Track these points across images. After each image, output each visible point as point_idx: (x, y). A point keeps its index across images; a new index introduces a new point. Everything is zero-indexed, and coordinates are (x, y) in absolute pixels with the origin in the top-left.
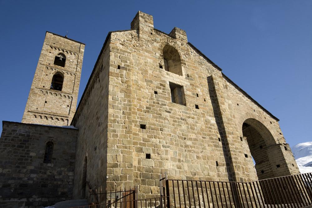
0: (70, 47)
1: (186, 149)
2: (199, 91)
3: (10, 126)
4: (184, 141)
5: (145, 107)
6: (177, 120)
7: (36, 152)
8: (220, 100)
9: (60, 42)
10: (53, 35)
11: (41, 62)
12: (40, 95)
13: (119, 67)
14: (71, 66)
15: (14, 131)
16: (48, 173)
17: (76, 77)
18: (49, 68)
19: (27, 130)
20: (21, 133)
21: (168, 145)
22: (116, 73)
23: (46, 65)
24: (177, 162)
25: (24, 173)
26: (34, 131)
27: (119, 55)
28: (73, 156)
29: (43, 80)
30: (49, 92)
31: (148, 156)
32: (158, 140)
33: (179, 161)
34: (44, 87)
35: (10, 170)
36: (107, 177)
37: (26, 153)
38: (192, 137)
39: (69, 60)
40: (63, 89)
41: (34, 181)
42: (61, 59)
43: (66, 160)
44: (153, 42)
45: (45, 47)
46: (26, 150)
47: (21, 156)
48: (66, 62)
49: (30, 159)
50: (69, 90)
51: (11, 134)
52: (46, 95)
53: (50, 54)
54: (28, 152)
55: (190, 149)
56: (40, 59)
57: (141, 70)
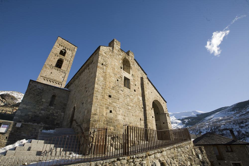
2: (136, 83)
3: (33, 83)
6: (126, 95)
7: (45, 100)
8: (145, 89)
9: (65, 43)
13: (102, 64)
15: (35, 86)
16: (51, 112)
17: (70, 63)
18: (56, 56)
19: (43, 87)
20: (39, 88)
21: (120, 107)
22: (101, 67)
23: (55, 54)
24: (124, 116)
26: (46, 88)
27: (103, 58)
28: (65, 105)
29: (52, 61)
30: (54, 68)
31: (111, 112)
32: (116, 104)
33: (125, 116)
34: (52, 65)
35: (30, 107)
36: (91, 120)
38: (131, 105)
39: (68, 54)
40: (62, 68)
41: (42, 115)
42: (64, 52)
43: (61, 106)
44: (119, 55)
45: (56, 44)
46: (40, 97)
47: (37, 100)
48: (66, 54)
49: (42, 102)
50: (65, 69)
51: (33, 87)
52: (52, 69)
56: (52, 50)
57: (112, 68)
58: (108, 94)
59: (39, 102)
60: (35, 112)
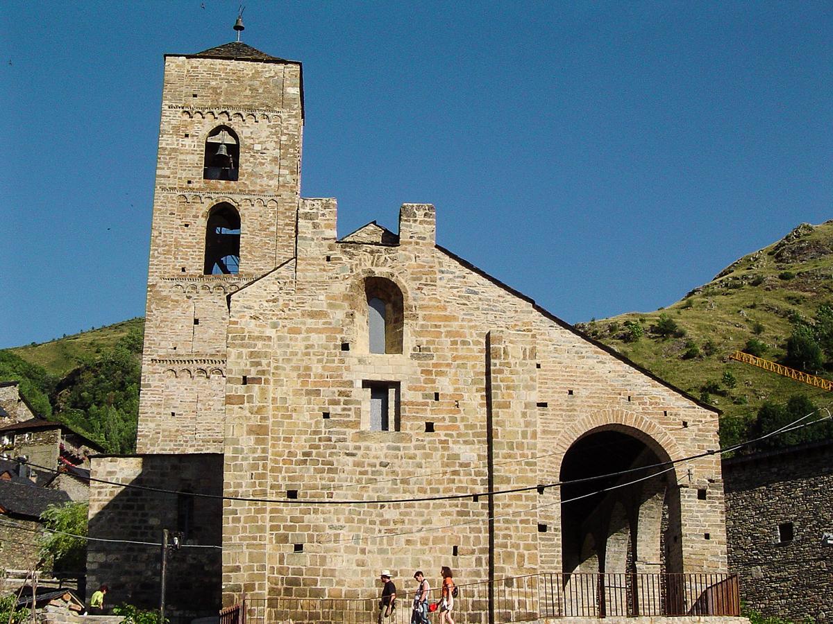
0: (248, 92)
1: (381, 527)
2: (445, 385)
4: (381, 511)
5: (299, 453)
6: (370, 469)
9: (213, 83)
10: (187, 60)
11: (162, 180)
12: (177, 301)
14: (258, 169)
15: (110, 473)
21: (340, 524)
24: (359, 554)
25: (144, 562)
29: (177, 244)
31: (299, 548)
33: (363, 551)
35: (119, 556)
36: (223, 587)
37: (140, 521)
45: (171, 118)
46: (140, 512)
47: (133, 527)
48: (243, 157)
50: (260, 265)
53: (188, 141)
54: (144, 518)
55: (392, 526)
56: (159, 172)
57: (297, 368)
58: (284, 489)
59: (139, 531)
60: (139, 573)
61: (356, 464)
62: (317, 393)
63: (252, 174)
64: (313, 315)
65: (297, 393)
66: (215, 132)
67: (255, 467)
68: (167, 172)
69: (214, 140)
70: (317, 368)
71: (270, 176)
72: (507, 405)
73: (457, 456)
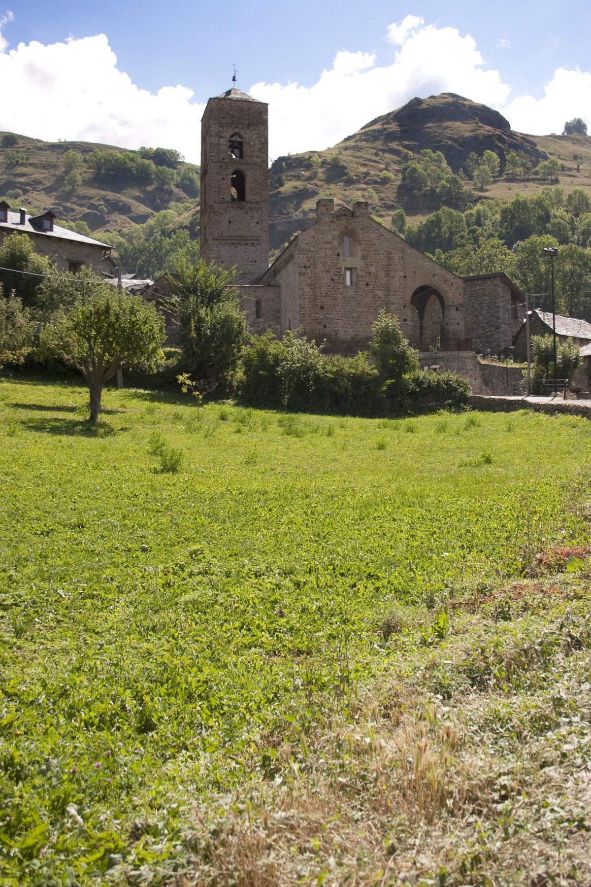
0: (246, 117)
2: (372, 269)
9: (231, 112)
13: (305, 267)
16: (261, 326)
28: (278, 311)
33: (346, 327)
53: (222, 140)
61: (344, 297)
62: (329, 272)
63: (250, 156)
64: (327, 243)
65: (322, 271)
66: (233, 136)
67: (310, 298)
68: (213, 154)
69: (233, 139)
70: (329, 263)
71: (257, 157)
72: (394, 277)
73: (377, 295)
